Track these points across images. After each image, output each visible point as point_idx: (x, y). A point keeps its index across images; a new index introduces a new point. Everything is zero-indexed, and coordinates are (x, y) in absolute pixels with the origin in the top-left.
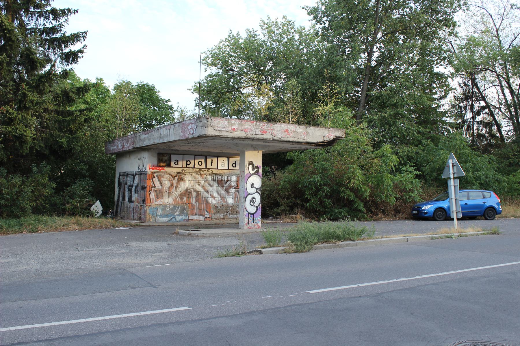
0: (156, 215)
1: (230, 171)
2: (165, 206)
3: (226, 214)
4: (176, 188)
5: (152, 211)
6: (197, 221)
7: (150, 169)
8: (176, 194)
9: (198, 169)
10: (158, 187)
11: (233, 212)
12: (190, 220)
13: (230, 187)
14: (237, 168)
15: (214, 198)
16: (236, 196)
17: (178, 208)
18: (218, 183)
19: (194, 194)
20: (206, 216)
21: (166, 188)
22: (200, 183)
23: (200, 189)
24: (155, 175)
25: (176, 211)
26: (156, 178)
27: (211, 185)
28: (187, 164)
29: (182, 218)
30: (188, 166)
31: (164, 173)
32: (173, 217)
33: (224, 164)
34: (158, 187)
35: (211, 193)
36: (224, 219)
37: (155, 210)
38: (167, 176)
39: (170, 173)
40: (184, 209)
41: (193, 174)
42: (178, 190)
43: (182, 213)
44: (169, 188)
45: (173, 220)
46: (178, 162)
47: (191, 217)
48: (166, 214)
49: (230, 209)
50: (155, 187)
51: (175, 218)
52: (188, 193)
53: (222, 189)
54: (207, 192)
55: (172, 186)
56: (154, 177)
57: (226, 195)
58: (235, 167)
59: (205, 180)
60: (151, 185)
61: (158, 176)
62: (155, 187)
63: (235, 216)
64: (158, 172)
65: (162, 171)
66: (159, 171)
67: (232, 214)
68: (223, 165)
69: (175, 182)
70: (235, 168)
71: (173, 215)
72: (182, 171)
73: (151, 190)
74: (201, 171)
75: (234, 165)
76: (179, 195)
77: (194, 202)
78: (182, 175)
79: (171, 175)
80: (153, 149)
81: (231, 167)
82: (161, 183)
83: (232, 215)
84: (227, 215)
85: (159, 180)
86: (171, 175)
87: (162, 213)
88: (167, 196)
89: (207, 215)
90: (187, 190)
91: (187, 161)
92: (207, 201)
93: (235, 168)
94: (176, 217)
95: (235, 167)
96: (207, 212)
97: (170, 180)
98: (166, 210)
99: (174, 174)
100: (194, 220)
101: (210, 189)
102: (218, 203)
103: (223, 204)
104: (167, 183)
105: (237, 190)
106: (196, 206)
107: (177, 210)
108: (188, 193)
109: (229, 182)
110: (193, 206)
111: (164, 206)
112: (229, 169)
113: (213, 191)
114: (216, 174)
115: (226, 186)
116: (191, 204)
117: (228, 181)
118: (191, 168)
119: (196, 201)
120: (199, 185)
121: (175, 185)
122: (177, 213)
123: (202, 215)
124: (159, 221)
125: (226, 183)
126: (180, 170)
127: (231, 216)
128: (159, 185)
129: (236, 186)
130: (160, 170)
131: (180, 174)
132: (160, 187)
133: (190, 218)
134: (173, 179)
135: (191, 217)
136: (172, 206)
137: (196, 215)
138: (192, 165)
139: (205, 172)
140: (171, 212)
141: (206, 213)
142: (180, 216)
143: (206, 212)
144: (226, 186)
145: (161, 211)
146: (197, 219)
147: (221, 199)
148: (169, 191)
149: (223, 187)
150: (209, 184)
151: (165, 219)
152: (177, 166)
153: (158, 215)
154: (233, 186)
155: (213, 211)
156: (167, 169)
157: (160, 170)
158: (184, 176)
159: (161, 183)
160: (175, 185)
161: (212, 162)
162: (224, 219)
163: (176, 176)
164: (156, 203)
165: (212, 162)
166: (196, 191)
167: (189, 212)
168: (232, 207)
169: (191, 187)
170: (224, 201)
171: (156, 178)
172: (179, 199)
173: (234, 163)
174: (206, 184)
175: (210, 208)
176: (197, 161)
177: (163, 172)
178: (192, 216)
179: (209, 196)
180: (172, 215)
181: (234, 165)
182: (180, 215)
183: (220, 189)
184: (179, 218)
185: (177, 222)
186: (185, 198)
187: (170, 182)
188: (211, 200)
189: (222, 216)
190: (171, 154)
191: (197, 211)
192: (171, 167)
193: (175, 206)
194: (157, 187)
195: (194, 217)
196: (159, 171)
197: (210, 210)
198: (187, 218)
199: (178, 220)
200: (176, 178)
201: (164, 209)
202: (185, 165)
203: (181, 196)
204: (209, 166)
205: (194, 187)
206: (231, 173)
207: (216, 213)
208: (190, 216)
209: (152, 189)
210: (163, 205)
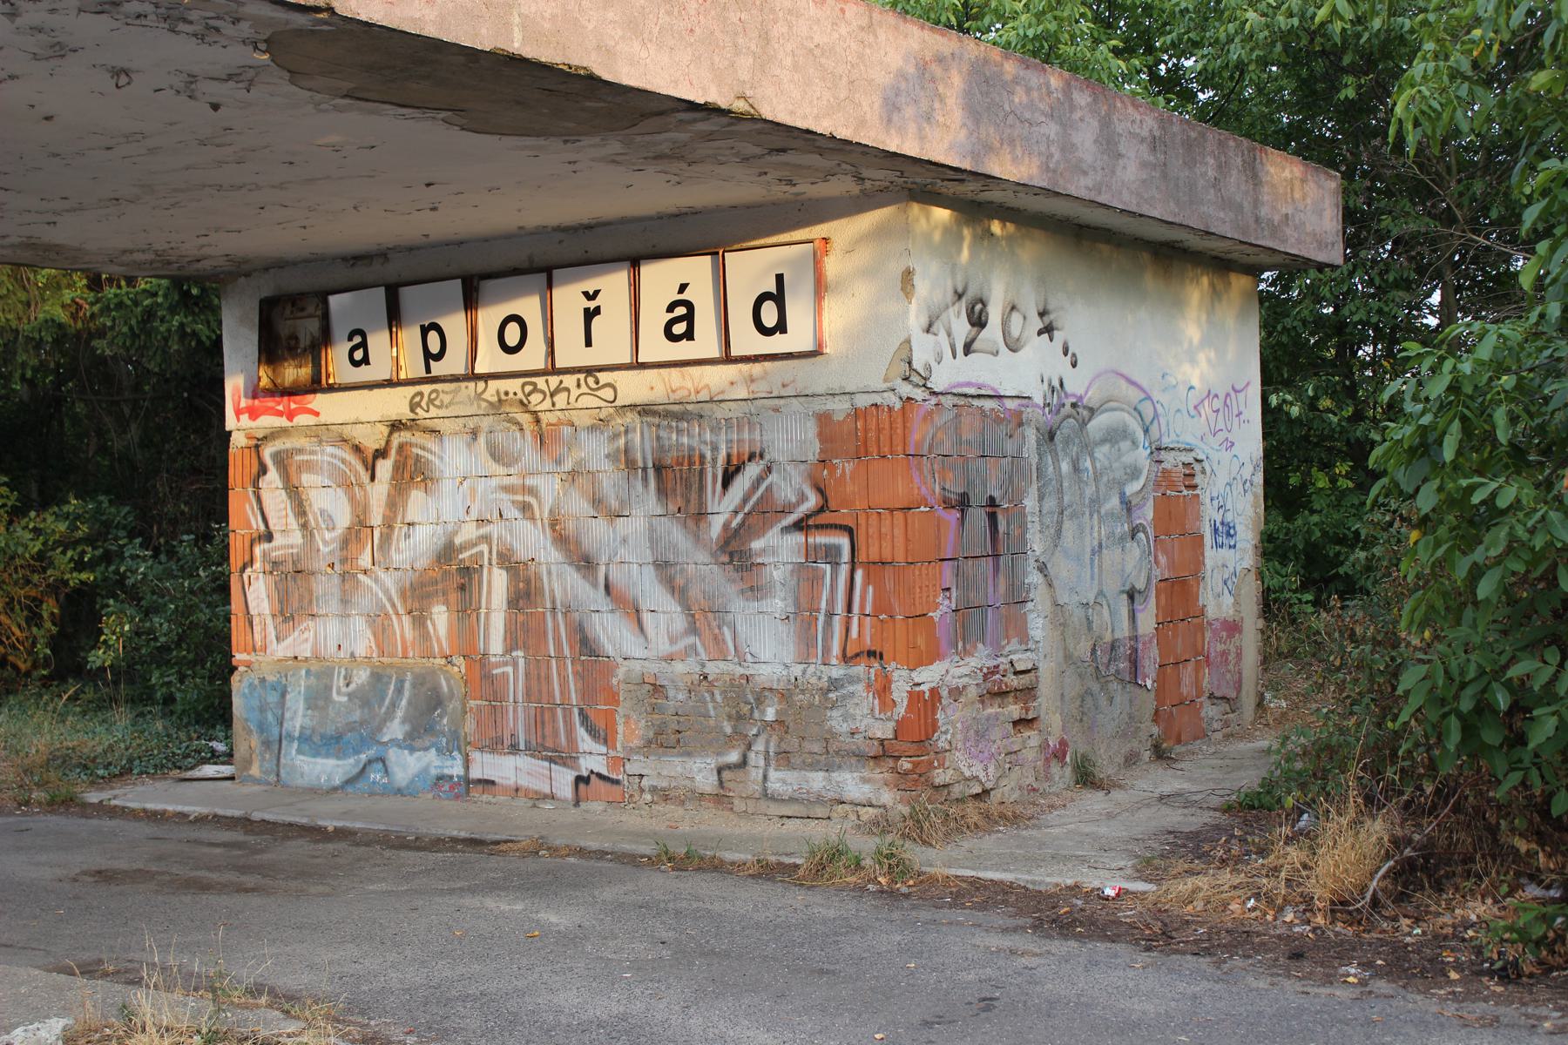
0: (275, 731)
1: (757, 368)
2: (322, 672)
3: (733, 757)
4: (386, 539)
5: (255, 703)
6: (522, 802)
7: (238, 412)
8: (381, 586)
9: (514, 385)
10: (288, 539)
11: (792, 742)
12: (476, 793)
13: (762, 512)
14: (797, 338)
15: (635, 613)
16: (814, 598)
17: (399, 691)
18: (662, 492)
19: (497, 584)
20: (588, 764)
21: (326, 543)
22: (532, 491)
23: (532, 542)
24: (267, 453)
25: (390, 715)
26: (273, 476)
27: (614, 504)
28: (428, 356)
29: (426, 770)
30: (438, 368)
31: (321, 433)
32: (372, 753)
33: (689, 318)
34: (288, 539)
35: (616, 575)
36: (721, 798)
37: (273, 698)
38: (330, 454)
39: (347, 431)
40: (435, 701)
41: (485, 423)
42: (397, 558)
43: (421, 731)
44: (345, 542)
45: (375, 775)
46: (364, 345)
47: (486, 765)
48: (330, 730)
49: (770, 714)
50: (269, 537)
51: (382, 760)
52: (458, 580)
53: (697, 539)
54: (586, 564)
55: (360, 525)
56: (263, 470)
57: (731, 590)
58: (781, 327)
59: (568, 466)
60: (250, 527)
61: (282, 460)
62: (269, 537)
63: (817, 781)
64: (282, 432)
65: (302, 420)
66: (282, 422)
67: (784, 758)
68: (679, 329)
69: (379, 492)
70: (777, 344)
71: (372, 738)
72: (413, 407)
73: (252, 562)
74: (535, 398)
75: (769, 316)
76: (403, 594)
77: (496, 646)
78: (419, 438)
79: (357, 449)
80: (247, 275)
81: (747, 340)
82: (300, 510)
83: (791, 776)
84: (743, 763)
85: (294, 491)
86: (357, 449)
87: (308, 722)
88: (334, 606)
89: (593, 759)
90: (447, 552)
91: (425, 331)
92: (586, 645)
93: (777, 344)
94: (393, 754)
95: (781, 327)
96: (593, 732)
97: (347, 485)
98: (328, 699)
99: (372, 439)
100: (505, 789)
101: (598, 533)
102: (670, 659)
103: (712, 669)
104: (332, 505)
105: (821, 539)
106: (513, 673)
107: (394, 705)
108: (458, 580)
109: (752, 470)
110: (488, 677)
111: (318, 676)
112: (728, 359)
113: (623, 553)
114: (645, 410)
115: (723, 509)
116: (479, 662)
117: (738, 470)
118: (455, 379)
119: (511, 644)
120: (525, 508)
121: (376, 519)
122: (396, 729)
123: (562, 757)
124: (300, 782)
125: (727, 481)
126: (395, 403)
127: (781, 781)
128: (293, 523)
129: (812, 501)
130: (290, 417)
131: (404, 436)
132: (297, 538)
133: (475, 773)
134: (365, 477)
135: (486, 765)
136: (362, 676)
137: (514, 749)
138: (454, 362)
139: (561, 400)
140: (357, 715)
141: (585, 741)
142: (412, 750)
143: (581, 732)
144: (723, 509)
145: (301, 705)
146: (524, 782)
147: (693, 629)
148: (344, 561)
149: (701, 515)
150: (597, 502)
151: (327, 769)
152: (363, 374)
153: (291, 737)
154: (785, 511)
155: (631, 728)
156: (327, 406)
157: (290, 417)
158: (430, 442)
159: (300, 510)
160: (376, 519)
161: (590, 315)
162: (721, 798)
163: (381, 454)
164: (280, 650)
165: (590, 315)
166: (507, 560)
167: (470, 726)
168: (785, 696)
169: (469, 532)
170: (718, 640)
171: (273, 476)
172: (406, 620)
173: (764, 297)
174: (577, 505)
175: (613, 698)
176: (489, 318)
177: (308, 431)
178: (488, 758)
179: (598, 598)
180: (364, 743)
181: (769, 316)
182: (411, 742)
183: (676, 534)
184: (408, 765)
185: (399, 792)
186: (441, 617)
187: (352, 499)
188: (612, 632)
189: (700, 772)
190: (323, 296)
191: (517, 721)
192: (332, 389)
193: (377, 677)
194: (278, 540)
195: (506, 769)
196: (282, 422)
197: (610, 716)
198: (456, 770)
199: (401, 776)
200: (385, 468)
201: (318, 699)
202: (413, 365)
203: (418, 595)
204: (571, 352)
205: (494, 530)
206: (761, 388)
207: (664, 741)
208: (476, 756)
209: (258, 550)
210: (315, 667)
